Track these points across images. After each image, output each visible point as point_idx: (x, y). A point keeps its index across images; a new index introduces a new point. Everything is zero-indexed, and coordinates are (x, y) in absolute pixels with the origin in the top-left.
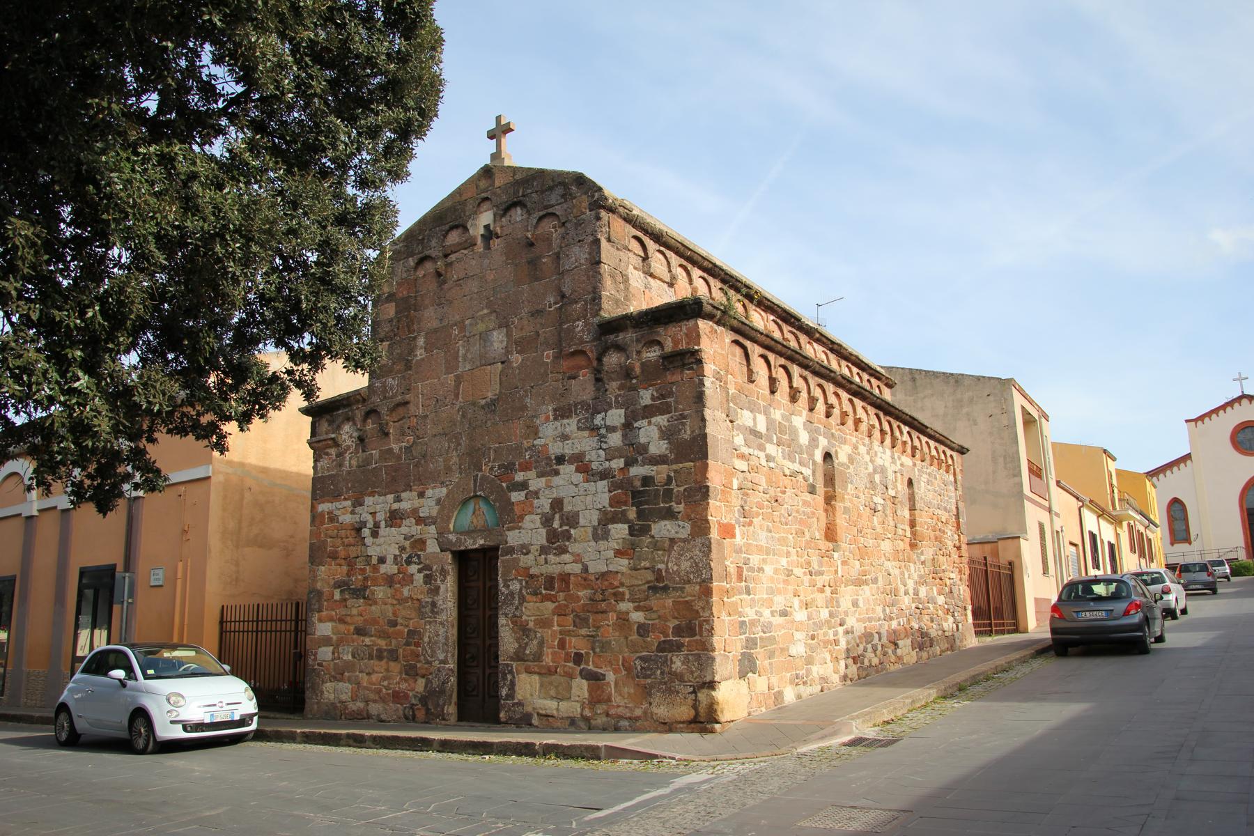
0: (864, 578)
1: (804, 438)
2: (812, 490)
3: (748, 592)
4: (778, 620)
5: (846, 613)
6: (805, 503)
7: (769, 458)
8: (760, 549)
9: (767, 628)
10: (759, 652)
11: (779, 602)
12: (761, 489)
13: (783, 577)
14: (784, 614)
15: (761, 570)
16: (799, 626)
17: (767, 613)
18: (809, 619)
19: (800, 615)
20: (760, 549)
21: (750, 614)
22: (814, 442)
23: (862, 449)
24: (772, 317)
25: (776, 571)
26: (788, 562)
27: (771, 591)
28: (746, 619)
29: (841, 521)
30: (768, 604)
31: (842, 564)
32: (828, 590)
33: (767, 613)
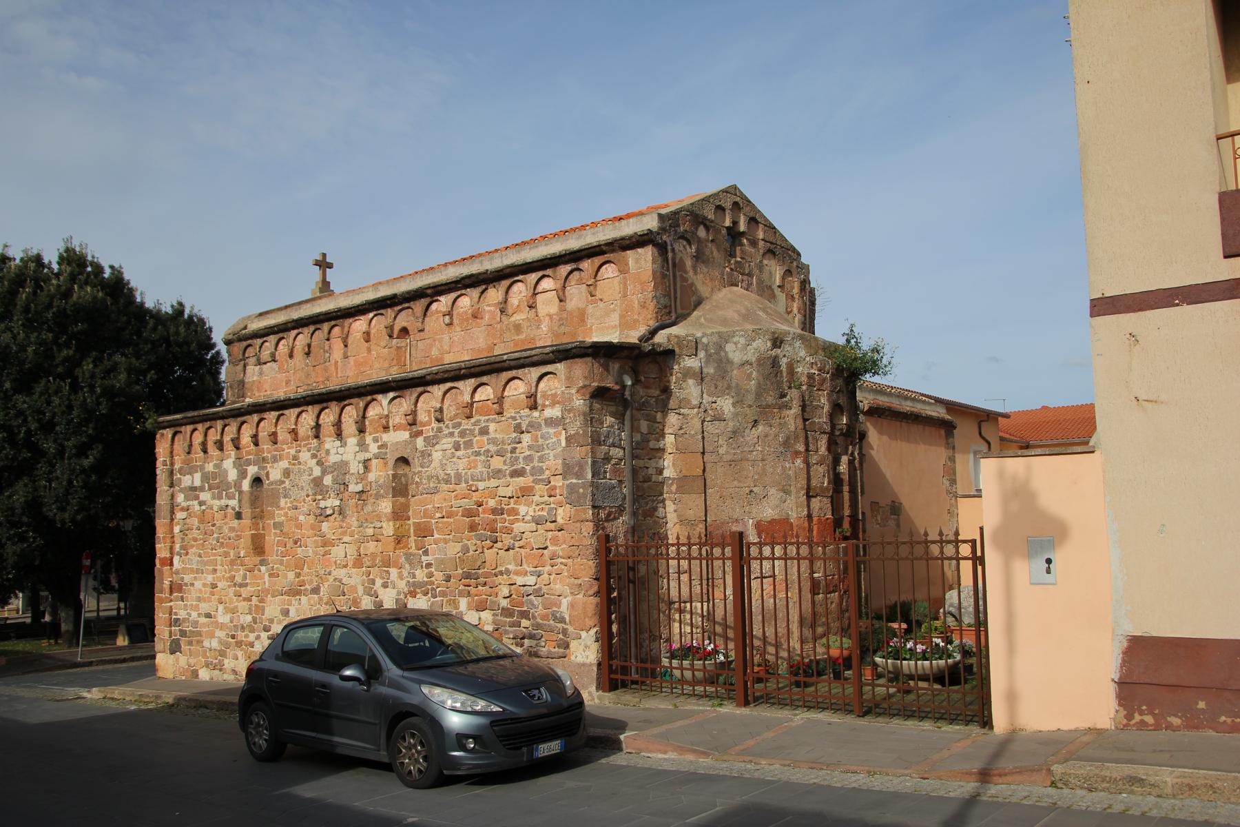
0: (302, 588)
1: (232, 475)
2: (239, 516)
3: (182, 599)
4: (203, 620)
5: (271, 621)
6: (232, 529)
7: (201, 504)
8: (192, 571)
9: (196, 623)
10: (183, 641)
11: (205, 607)
12: (195, 527)
13: (209, 589)
14: (208, 616)
15: (192, 585)
16: (222, 627)
17: (194, 614)
18: (232, 622)
19: (223, 618)
20: (192, 571)
21: (182, 614)
22: (243, 474)
23: (305, 456)
24: (371, 315)
25: (204, 585)
26: (214, 578)
27: (199, 599)
28: (181, 617)
29: (272, 538)
30: (196, 608)
31: (269, 577)
32: (255, 600)
33: (194, 614)
